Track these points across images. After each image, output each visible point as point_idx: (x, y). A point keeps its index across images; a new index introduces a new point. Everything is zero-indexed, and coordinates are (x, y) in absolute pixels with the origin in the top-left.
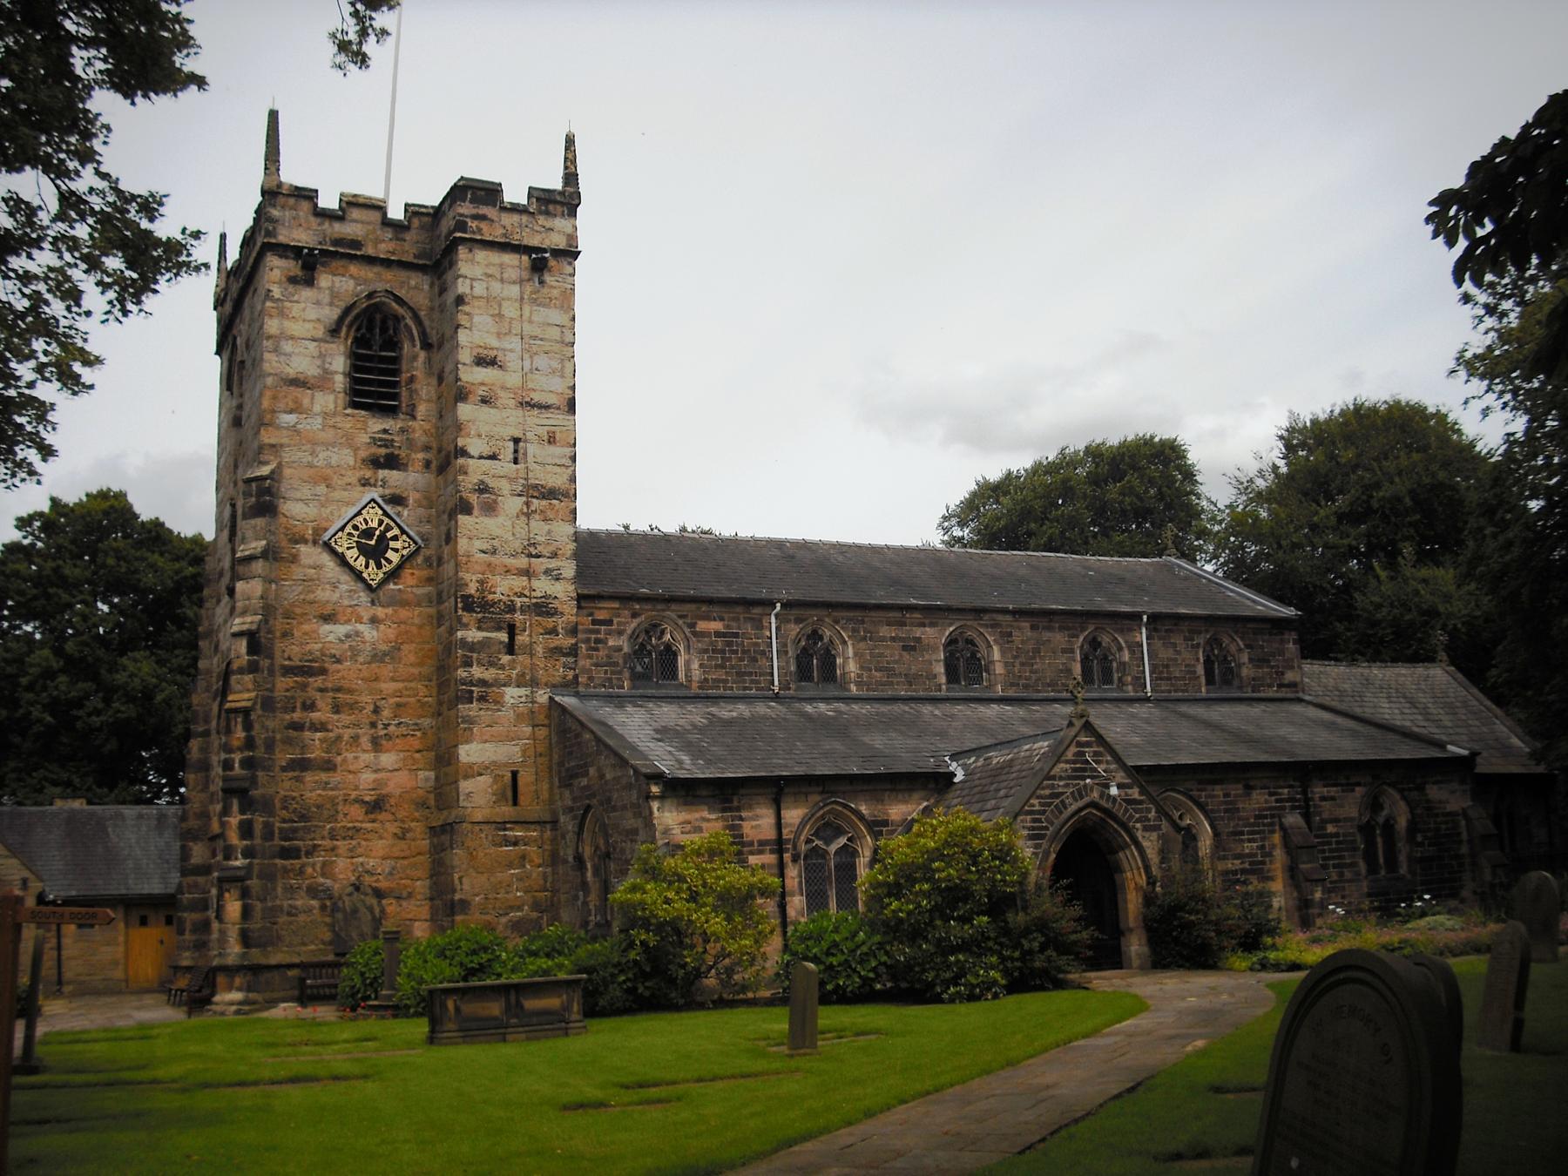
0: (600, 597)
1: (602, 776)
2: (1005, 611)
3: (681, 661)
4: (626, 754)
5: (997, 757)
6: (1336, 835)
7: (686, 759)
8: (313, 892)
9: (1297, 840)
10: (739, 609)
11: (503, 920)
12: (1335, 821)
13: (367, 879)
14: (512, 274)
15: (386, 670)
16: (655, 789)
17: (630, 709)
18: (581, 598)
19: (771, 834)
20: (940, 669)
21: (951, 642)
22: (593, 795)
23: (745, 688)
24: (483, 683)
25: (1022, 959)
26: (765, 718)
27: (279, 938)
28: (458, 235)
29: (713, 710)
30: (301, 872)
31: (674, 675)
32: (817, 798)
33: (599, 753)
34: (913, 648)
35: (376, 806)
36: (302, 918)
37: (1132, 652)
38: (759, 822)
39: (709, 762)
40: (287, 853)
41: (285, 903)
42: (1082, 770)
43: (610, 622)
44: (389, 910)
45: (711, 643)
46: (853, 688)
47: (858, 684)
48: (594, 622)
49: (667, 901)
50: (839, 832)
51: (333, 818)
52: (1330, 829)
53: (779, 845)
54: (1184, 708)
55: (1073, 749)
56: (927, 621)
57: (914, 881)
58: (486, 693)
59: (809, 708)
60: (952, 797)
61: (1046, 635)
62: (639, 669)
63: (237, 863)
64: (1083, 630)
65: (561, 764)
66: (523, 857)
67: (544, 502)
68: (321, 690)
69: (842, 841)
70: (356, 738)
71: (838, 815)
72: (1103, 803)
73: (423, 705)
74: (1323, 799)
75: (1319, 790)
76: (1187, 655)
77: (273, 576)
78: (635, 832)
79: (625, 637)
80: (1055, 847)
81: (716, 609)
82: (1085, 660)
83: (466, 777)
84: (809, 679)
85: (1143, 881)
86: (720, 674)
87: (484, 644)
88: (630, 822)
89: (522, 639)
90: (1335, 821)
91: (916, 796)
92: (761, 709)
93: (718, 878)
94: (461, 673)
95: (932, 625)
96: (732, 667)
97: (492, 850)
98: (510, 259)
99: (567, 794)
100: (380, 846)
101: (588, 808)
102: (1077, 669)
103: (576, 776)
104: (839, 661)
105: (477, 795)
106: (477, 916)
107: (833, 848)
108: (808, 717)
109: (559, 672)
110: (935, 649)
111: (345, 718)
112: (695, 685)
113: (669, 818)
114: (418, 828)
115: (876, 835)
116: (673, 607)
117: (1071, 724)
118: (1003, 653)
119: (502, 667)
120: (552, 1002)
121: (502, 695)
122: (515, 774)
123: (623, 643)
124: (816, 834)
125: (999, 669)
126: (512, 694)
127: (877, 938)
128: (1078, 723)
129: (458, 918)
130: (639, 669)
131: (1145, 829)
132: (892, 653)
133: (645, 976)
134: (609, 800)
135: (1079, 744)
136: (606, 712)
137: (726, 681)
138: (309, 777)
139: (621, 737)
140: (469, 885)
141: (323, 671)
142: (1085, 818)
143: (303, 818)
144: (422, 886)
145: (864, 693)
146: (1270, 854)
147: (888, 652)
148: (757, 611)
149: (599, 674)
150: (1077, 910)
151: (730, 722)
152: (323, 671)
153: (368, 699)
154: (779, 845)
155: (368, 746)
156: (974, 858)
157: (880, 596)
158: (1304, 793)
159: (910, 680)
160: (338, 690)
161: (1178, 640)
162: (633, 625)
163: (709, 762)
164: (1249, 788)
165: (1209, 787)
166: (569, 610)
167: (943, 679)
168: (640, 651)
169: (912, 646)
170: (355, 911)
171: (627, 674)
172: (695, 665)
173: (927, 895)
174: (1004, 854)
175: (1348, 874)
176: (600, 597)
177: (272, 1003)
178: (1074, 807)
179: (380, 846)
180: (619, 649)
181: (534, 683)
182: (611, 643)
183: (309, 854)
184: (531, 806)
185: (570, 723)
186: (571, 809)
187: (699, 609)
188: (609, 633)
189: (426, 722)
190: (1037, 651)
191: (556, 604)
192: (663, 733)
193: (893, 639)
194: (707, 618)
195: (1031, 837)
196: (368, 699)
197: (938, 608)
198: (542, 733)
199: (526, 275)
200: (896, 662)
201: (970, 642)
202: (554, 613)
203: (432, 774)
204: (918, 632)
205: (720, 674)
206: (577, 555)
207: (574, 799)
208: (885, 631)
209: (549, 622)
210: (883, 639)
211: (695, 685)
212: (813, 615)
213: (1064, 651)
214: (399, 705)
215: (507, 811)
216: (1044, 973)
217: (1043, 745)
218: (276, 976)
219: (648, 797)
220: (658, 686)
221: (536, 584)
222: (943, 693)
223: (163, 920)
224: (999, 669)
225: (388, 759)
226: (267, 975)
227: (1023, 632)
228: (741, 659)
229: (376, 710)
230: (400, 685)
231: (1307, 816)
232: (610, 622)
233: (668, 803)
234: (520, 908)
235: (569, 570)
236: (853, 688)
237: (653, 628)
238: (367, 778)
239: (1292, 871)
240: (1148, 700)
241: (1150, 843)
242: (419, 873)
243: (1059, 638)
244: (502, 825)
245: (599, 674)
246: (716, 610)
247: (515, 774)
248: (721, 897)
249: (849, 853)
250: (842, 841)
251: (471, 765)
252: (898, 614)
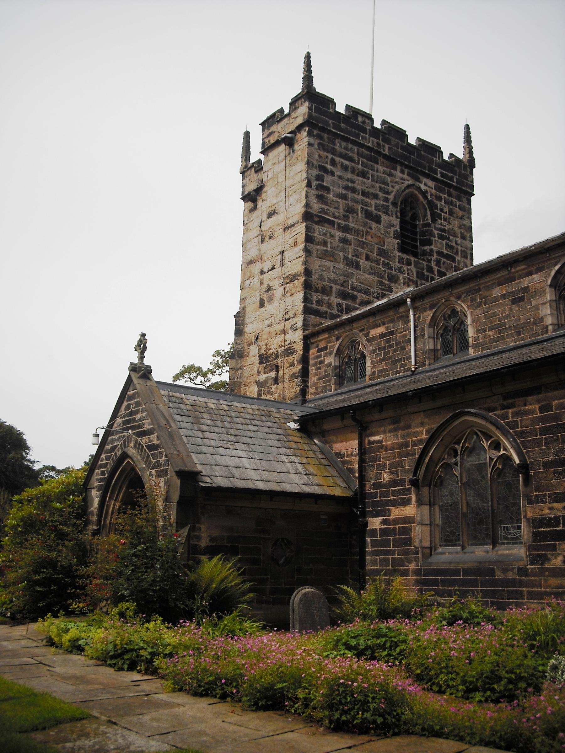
10: (391, 313)
23: (397, 372)
34: (522, 299)
56: (534, 269)
67: (291, 284)
77: (239, 366)
81: (378, 317)
95: (539, 270)
96: (390, 358)
116: (355, 325)
137: (385, 370)
145: (481, 353)
147: (498, 311)
162: (337, 346)
165: (519, 401)
182: (327, 362)
187: (369, 321)
193: (504, 296)
194: (375, 326)
200: (507, 317)
204: (526, 282)
208: (497, 292)
210: (496, 299)
212: (441, 297)
228: (395, 351)
252: (503, 273)
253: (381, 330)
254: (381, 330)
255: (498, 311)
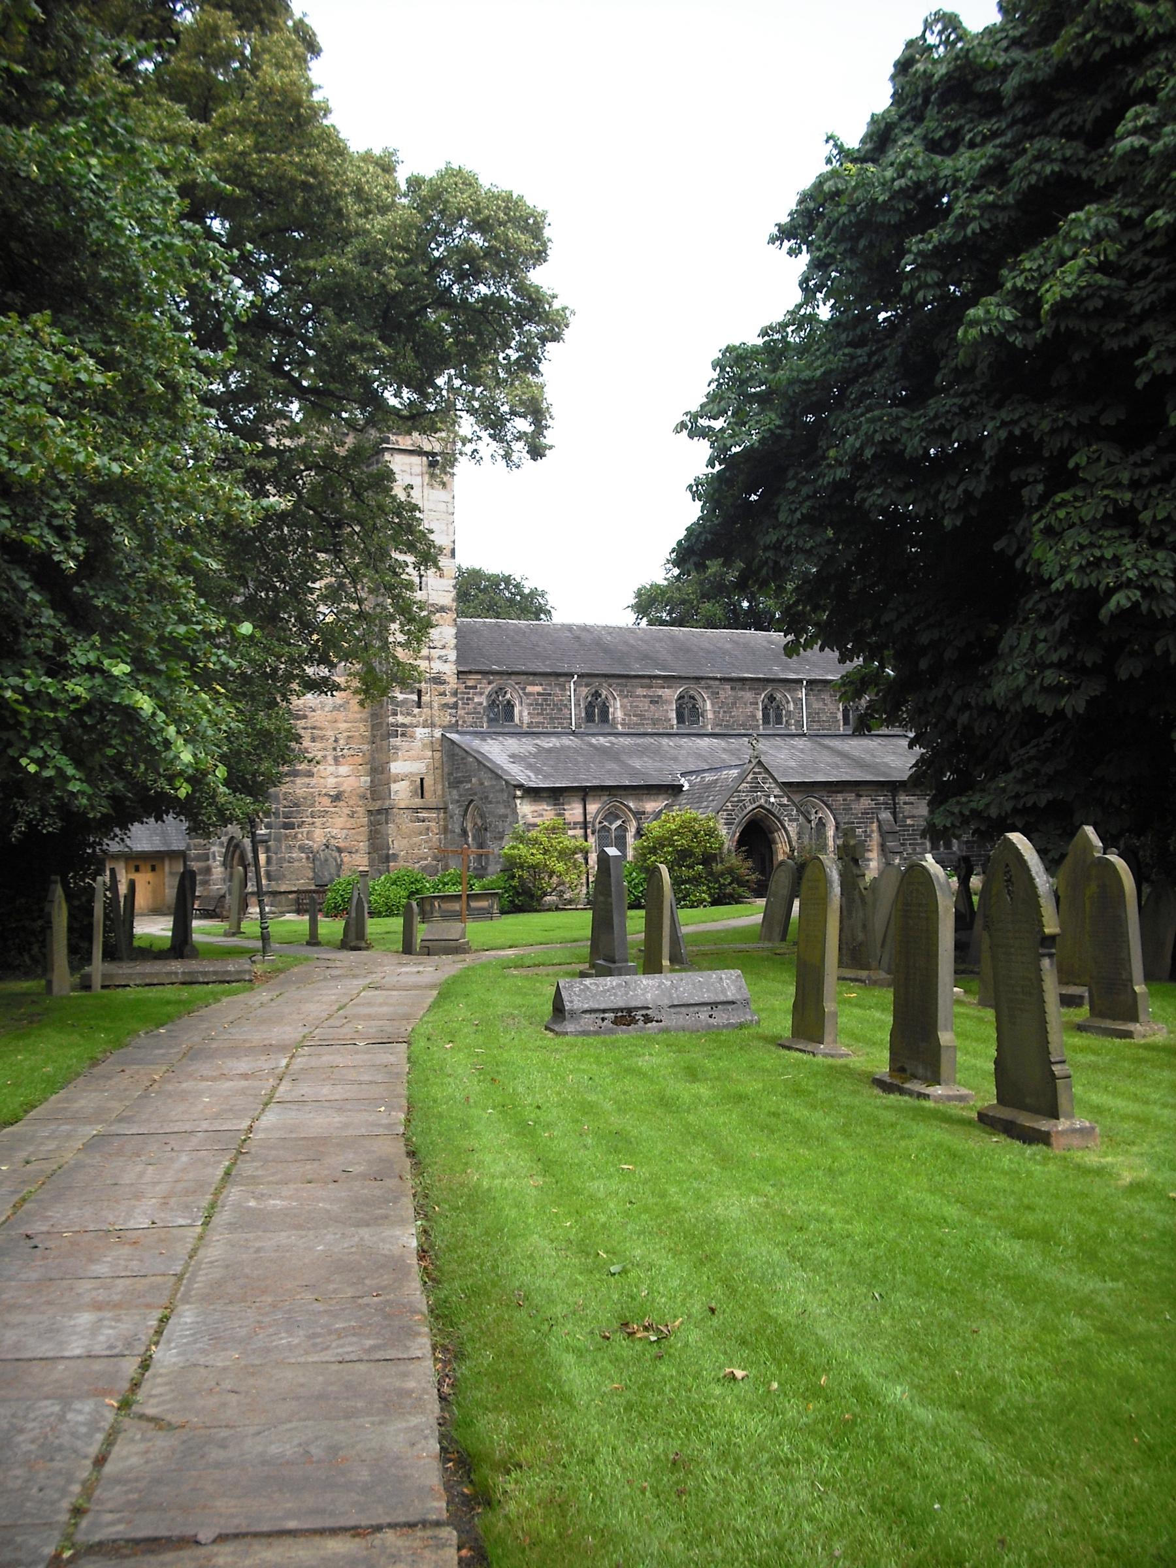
0: (470, 672)
1: (482, 784)
2: (715, 679)
3: (516, 710)
4: (500, 772)
5: (709, 777)
6: (913, 825)
7: (531, 775)
8: (302, 849)
9: (886, 828)
10: (552, 679)
11: (417, 865)
12: (913, 817)
13: (332, 841)
14: (417, 469)
15: (341, 716)
16: (519, 793)
17: (490, 741)
18: (459, 673)
19: (581, 819)
20: (673, 715)
21: (681, 697)
22: (475, 794)
24: (403, 725)
25: (719, 888)
26: (569, 747)
27: (284, 876)
28: (385, 445)
29: (538, 741)
30: (295, 837)
31: (512, 719)
32: (606, 798)
33: (479, 770)
34: (657, 702)
35: (337, 798)
36: (296, 864)
37: (795, 704)
38: (574, 812)
39: (546, 777)
40: (287, 826)
41: (287, 856)
42: (756, 787)
43: (476, 687)
44: (345, 859)
45: (536, 700)
46: (619, 727)
47: (622, 724)
48: (466, 687)
49: (532, 854)
50: (617, 817)
51: (312, 805)
52: (909, 822)
53: (585, 825)
54: (827, 742)
55: (751, 776)
57: (664, 846)
58: (404, 732)
59: (593, 740)
60: (683, 799)
61: (741, 693)
62: (492, 715)
63: (262, 832)
64: (764, 690)
65: (450, 774)
66: (428, 829)
68: (304, 728)
69: (619, 822)
70: (324, 757)
71: (617, 808)
72: (767, 806)
73: (363, 737)
74: (905, 803)
75: (903, 798)
76: (832, 707)
78: (506, 816)
79: (484, 697)
80: (740, 829)
82: (765, 709)
83: (395, 782)
84: (593, 721)
85: (787, 849)
86: (540, 719)
87: (405, 702)
88: (502, 811)
89: (425, 699)
90: (913, 817)
91: (661, 797)
92: (566, 741)
93: (560, 843)
94: (391, 720)
97: (411, 825)
98: (416, 460)
99: (455, 792)
100: (340, 821)
101: (472, 801)
102: (760, 715)
103: (461, 782)
104: (611, 710)
105: (401, 792)
106: (402, 863)
107: (614, 826)
108: (591, 745)
109: (447, 719)
110: (670, 703)
111: (318, 745)
112: (525, 726)
113: (526, 809)
114: (361, 811)
115: (638, 820)
116: (513, 677)
117: (750, 761)
118: (713, 705)
119: (415, 716)
120: (484, 904)
121: (414, 732)
122: (422, 780)
123: (483, 700)
124: (604, 819)
125: (710, 715)
126: (420, 732)
127: (643, 876)
128: (754, 761)
129: (392, 864)
130: (492, 715)
131: (790, 820)
132: (644, 705)
133: (518, 894)
134: (487, 798)
135: (755, 773)
136: (476, 743)
138: (299, 781)
139: (494, 763)
140: (398, 845)
141: (305, 717)
142: (756, 814)
143: (296, 805)
144: (363, 846)
145: (626, 730)
146: (870, 836)
148: (562, 679)
149: (469, 719)
150: (750, 864)
151: (549, 750)
152: (305, 717)
153: (331, 733)
154: (585, 825)
155: (332, 762)
156: (696, 834)
157: (637, 669)
158: (894, 800)
159: (655, 722)
160: (314, 728)
161: (826, 696)
163: (544, 776)
164: (859, 796)
166: (452, 680)
167: (675, 722)
168: (493, 704)
169: (656, 701)
170: (326, 860)
171: (485, 719)
172: (525, 713)
173: (670, 853)
174: (711, 833)
175: (918, 849)
176: (470, 672)
177: (283, 913)
178: (750, 808)
179: (340, 821)
180: (481, 704)
181: (433, 725)
182: (476, 700)
183: (299, 826)
184: (431, 799)
185: (457, 750)
186: (458, 801)
188: (475, 694)
189: (365, 747)
190: (734, 704)
191: (445, 677)
192: (514, 758)
193: (644, 696)
195: (726, 824)
196: (331, 733)
197: (673, 677)
198: (438, 755)
199: (425, 469)
201: (693, 698)
202: (444, 683)
203: (369, 779)
204: (660, 692)
205: (540, 719)
206: (457, 647)
207: (460, 796)
208: (640, 691)
209: (441, 688)
210: (638, 696)
211: (525, 726)
213: (751, 704)
214: (349, 737)
215: (418, 802)
216: (731, 896)
217: (734, 772)
218: (283, 897)
219: (515, 797)
220: (503, 726)
221: (433, 665)
222: (675, 731)
223: (149, 868)
224: (710, 715)
225: (344, 770)
226: (279, 897)
227: (726, 692)
229: (336, 741)
230: (350, 725)
231: (894, 814)
232: (476, 687)
233: (525, 800)
234: (426, 859)
235: (452, 655)
236: (619, 727)
237: (500, 691)
238: (331, 781)
239: (883, 846)
240: (804, 735)
241: (792, 828)
242: (361, 838)
243: (748, 695)
244: (416, 810)
245: (469, 719)
246: (538, 679)
247: (422, 780)
248: (560, 853)
249: (623, 829)
250: (619, 822)
251: (397, 775)
252: (647, 681)
253: (538, 689)
254: (538, 689)
255: (641, 705)
